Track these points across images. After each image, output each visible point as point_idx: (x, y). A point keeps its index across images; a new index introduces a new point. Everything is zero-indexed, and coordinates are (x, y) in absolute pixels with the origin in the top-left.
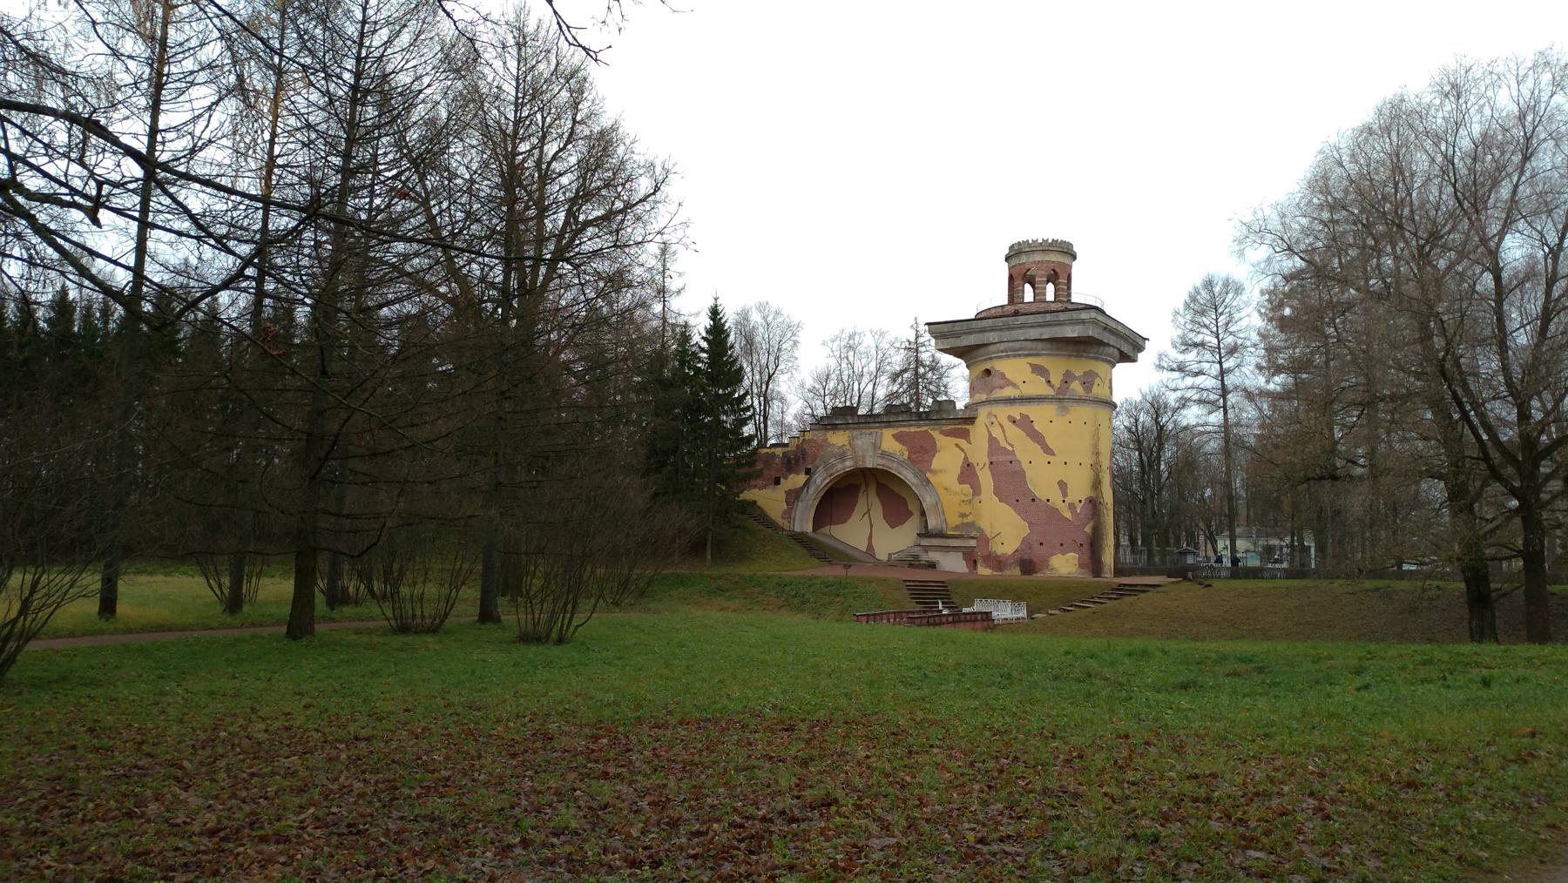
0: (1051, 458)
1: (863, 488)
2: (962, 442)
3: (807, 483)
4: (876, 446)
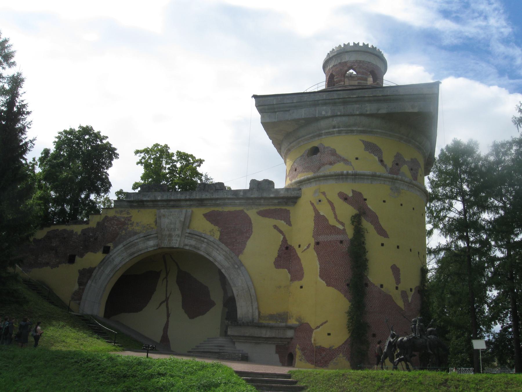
1: (163, 275)
2: (281, 224)
3: (103, 262)
4: (186, 224)
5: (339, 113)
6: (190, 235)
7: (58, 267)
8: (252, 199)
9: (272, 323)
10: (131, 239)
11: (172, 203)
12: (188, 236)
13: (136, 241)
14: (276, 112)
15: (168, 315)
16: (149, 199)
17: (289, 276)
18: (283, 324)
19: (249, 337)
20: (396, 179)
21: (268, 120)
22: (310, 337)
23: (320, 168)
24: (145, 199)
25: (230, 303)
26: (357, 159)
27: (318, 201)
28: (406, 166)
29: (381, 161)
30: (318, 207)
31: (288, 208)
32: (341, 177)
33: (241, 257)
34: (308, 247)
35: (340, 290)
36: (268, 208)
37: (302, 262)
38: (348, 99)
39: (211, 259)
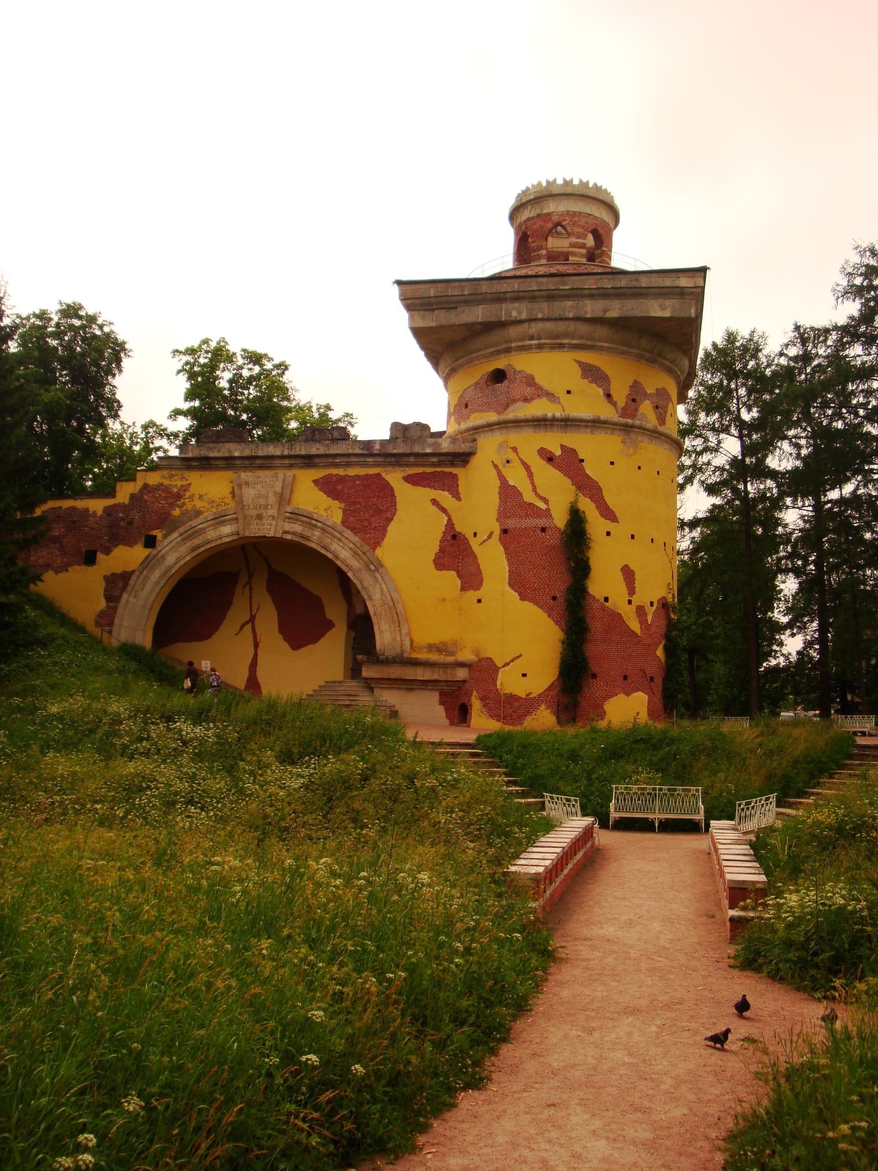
1: (243, 579)
2: (445, 497)
3: (147, 563)
4: (283, 499)
5: (540, 316)
6: (293, 516)
7: (67, 570)
8: (394, 455)
9: (434, 657)
10: (193, 523)
11: (259, 462)
12: (289, 518)
13: (201, 526)
14: (434, 310)
15: (256, 645)
16: (220, 455)
17: (459, 582)
18: (450, 659)
19: (396, 679)
20: (632, 426)
21: (420, 324)
22: (495, 680)
23: (508, 406)
24: (212, 455)
25: (361, 628)
26: (569, 392)
27: (504, 461)
28: (648, 401)
29: (609, 396)
30: (504, 472)
31: (454, 470)
32: (542, 423)
33: (379, 552)
34: (490, 536)
35: (541, 608)
36: (420, 470)
37: (480, 560)
38: (555, 292)
39: (329, 555)
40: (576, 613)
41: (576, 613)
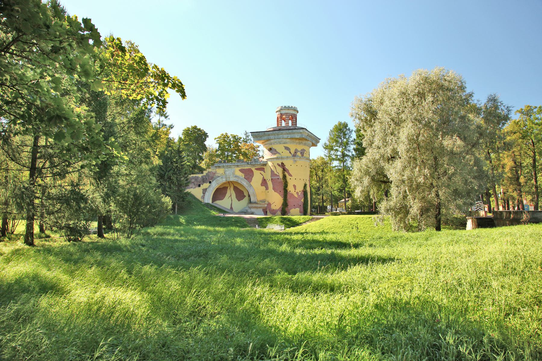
0: (290, 177)
1: (229, 188)
2: (262, 172)
4: (233, 173)
40: (285, 193)
41: (285, 193)
